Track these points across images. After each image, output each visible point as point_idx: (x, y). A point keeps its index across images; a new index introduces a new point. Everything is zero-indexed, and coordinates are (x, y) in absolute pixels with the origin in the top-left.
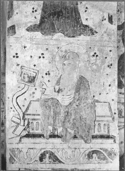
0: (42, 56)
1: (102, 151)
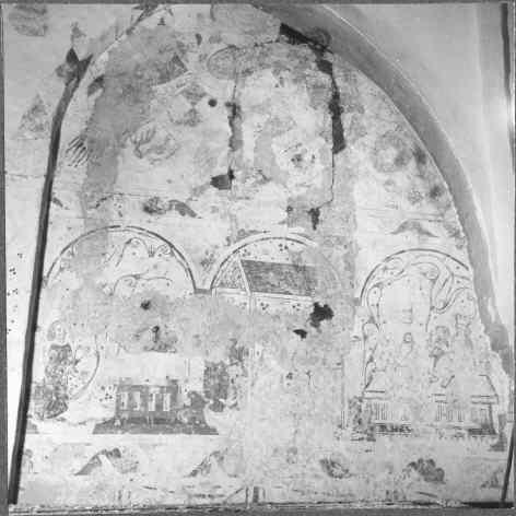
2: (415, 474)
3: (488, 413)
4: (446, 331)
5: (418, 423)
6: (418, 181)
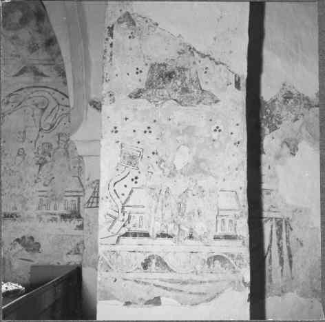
0: (148, 130)
1: (227, 257)
2: (19, 247)
3: (77, 202)
4: (50, 146)
5: (24, 211)
6: (37, 35)
